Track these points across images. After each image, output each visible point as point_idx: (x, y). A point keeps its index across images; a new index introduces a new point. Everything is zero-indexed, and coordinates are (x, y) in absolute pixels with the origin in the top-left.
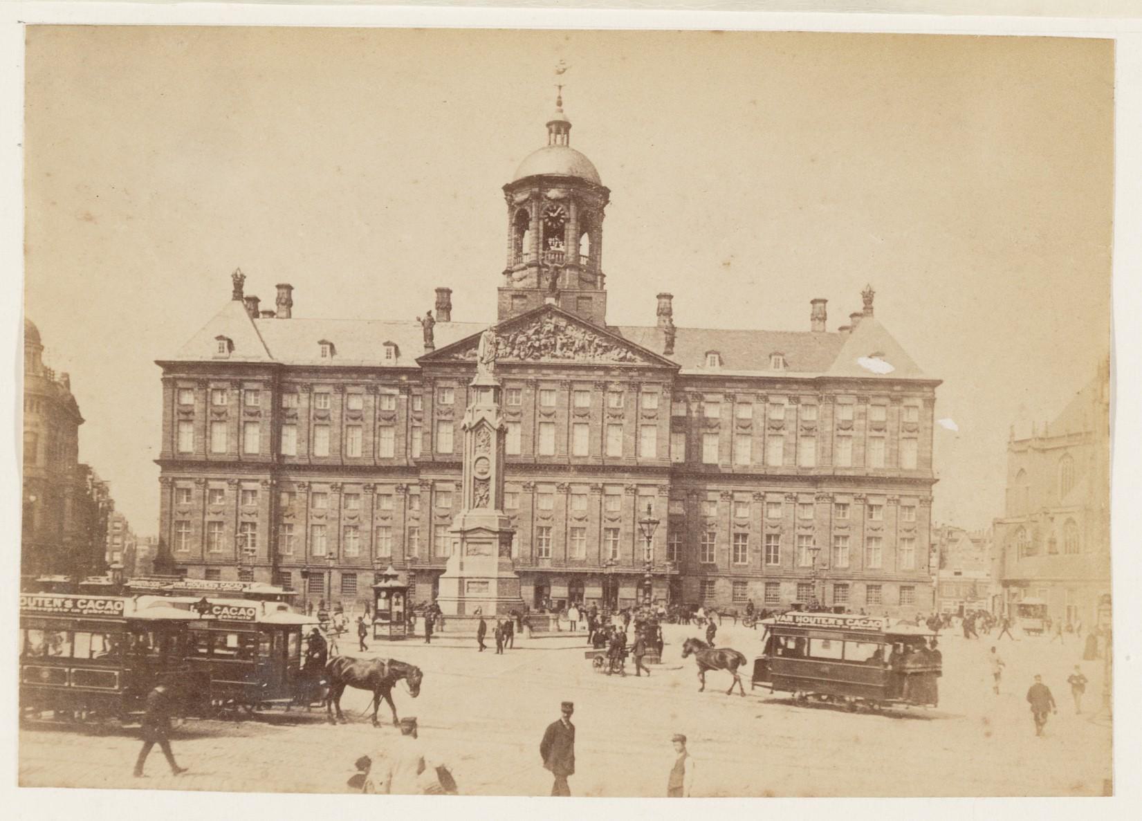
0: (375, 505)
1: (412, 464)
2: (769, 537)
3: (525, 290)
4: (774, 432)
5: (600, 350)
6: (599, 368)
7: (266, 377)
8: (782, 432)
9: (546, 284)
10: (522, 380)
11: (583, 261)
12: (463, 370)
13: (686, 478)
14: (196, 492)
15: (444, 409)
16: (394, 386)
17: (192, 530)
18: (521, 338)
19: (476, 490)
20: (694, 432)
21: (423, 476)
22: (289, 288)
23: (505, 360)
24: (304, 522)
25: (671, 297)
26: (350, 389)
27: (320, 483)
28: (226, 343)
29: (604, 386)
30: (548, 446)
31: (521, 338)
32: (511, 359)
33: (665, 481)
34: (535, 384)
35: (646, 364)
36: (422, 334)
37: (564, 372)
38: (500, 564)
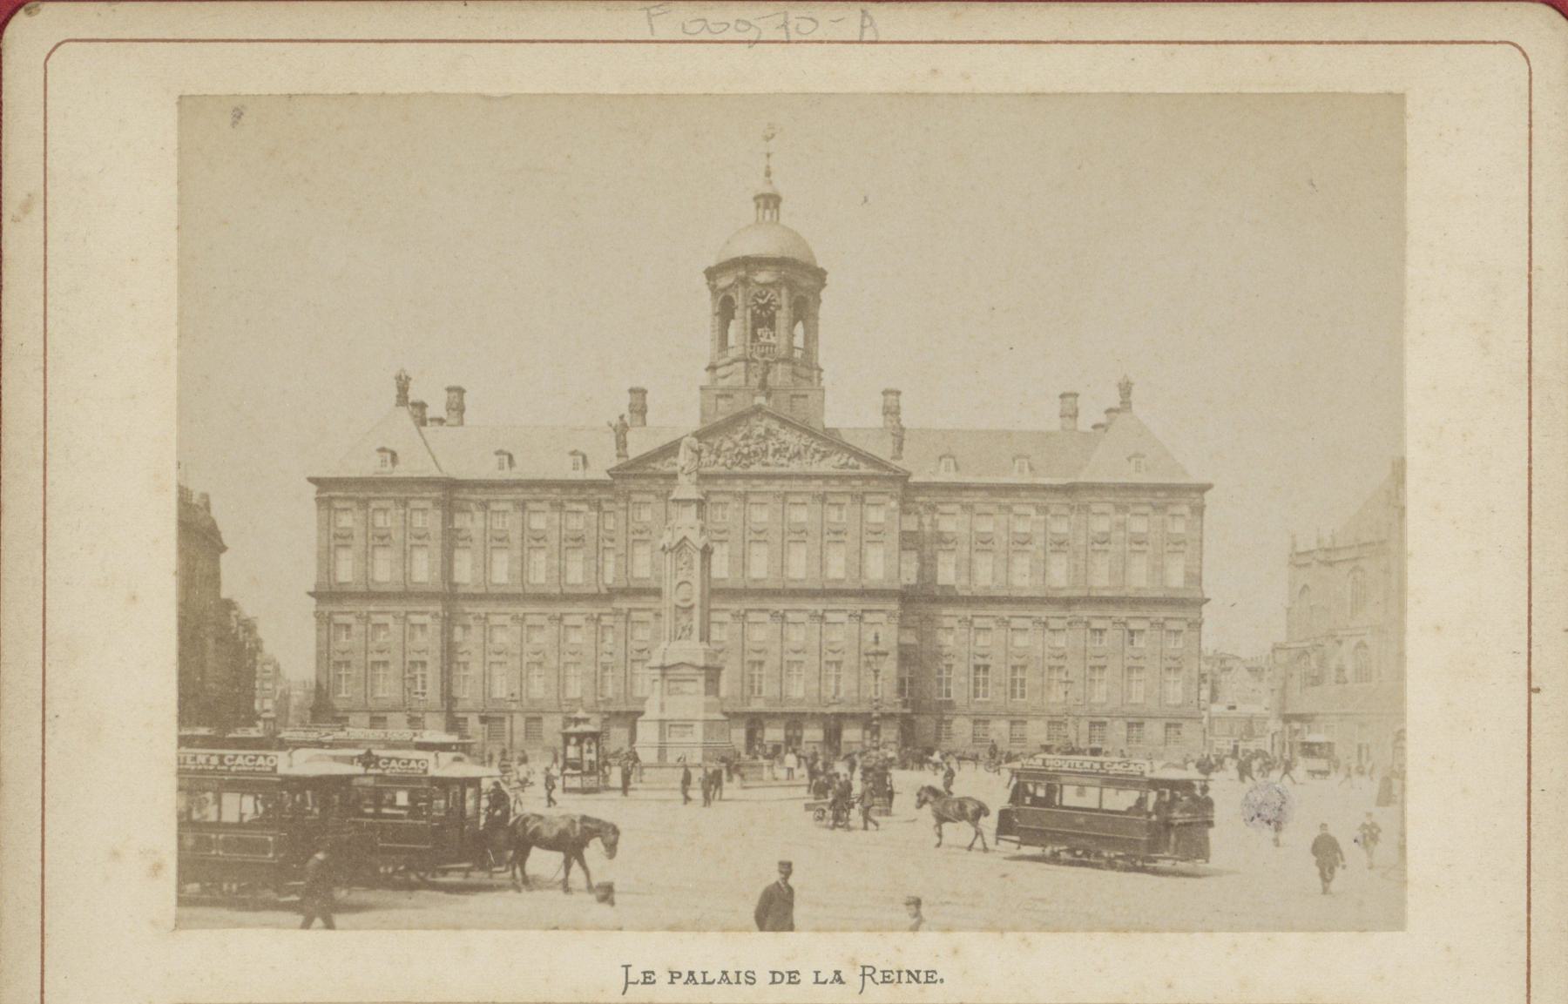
1: (604, 591)
2: (1014, 668)
3: (729, 388)
4: (1020, 547)
5: (818, 456)
6: (817, 477)
7: (435, 495)
8: (1028, 547)
11: (798, 354)
13: (918, 601)
14: (357, 628)
15: (640, 527)
16: (585, 500)
17: (354, 672)
18: (728, 444)
19: (677, 619)
20: (927, 548)
21: (617, 604)
22: (461, 391)
23: (709, 470)
25: (898, 393)
27: (500, 615)
28: (388, 456)
30: (760, 568)
31: (728, 444)
33: (894, 606)
34: (744, 497)
35: (872, 471)
36: (613, 441)
37: (779, 482)
38: (706, 704)
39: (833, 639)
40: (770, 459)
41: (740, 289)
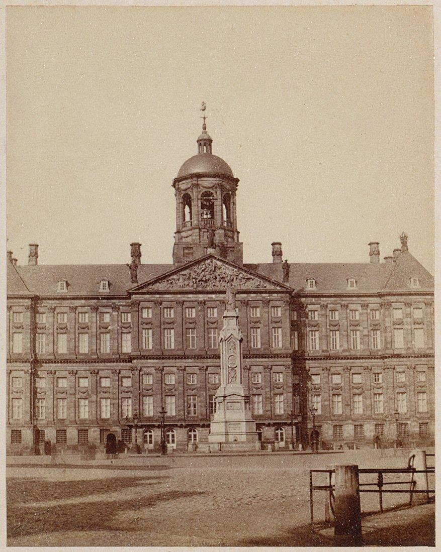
0: (98, 383)
9: (205, 240)
12: (158, 296)
24: (52, 397)
25: (280, 244)
29: (267, 303)
32: (187, 289)
33: (289, 361)
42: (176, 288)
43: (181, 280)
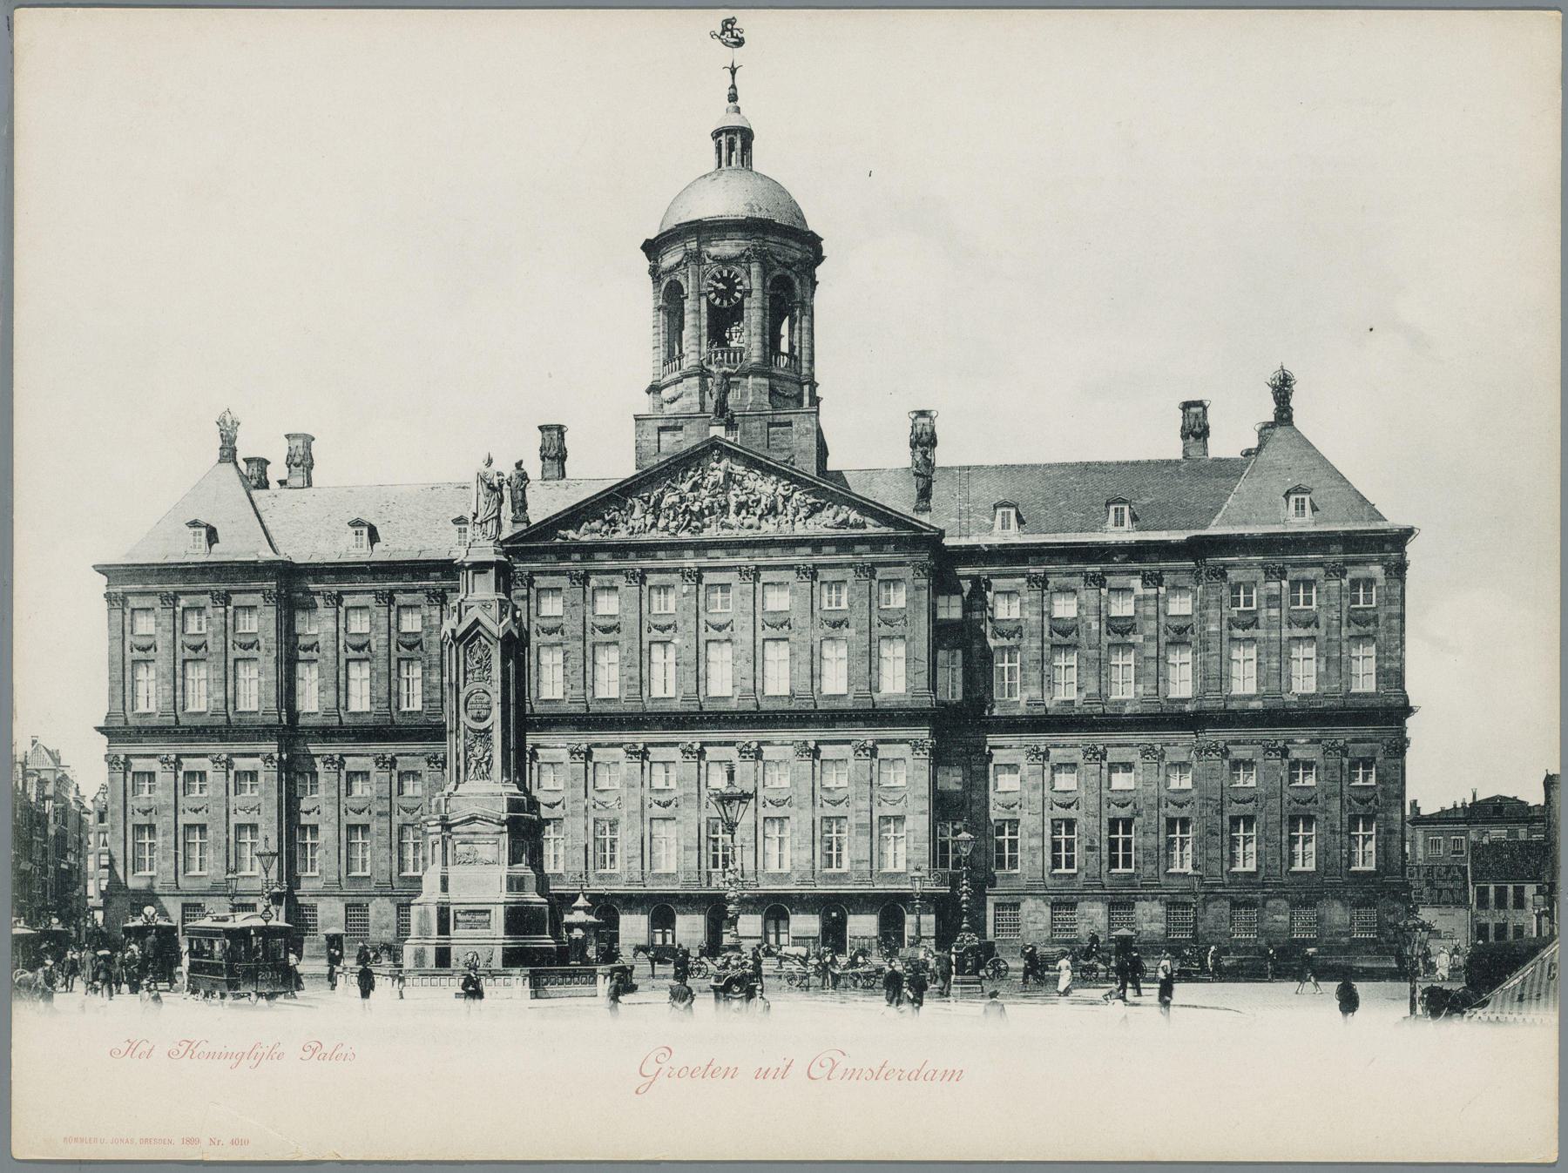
5: (803, 512)
9: (711, 404)
10: (676, 570)
14: (164, 777)
18: (671, 498)
26: (401, 599)
27: (360, 758)
30: (609, 683)
32: (654, 536)
33: (923, 734)
37: (745, 552)
39: (831, 784)
40: (732, 519)
41: (692, 267)
42: (622, 535)
43: (637, 513)
